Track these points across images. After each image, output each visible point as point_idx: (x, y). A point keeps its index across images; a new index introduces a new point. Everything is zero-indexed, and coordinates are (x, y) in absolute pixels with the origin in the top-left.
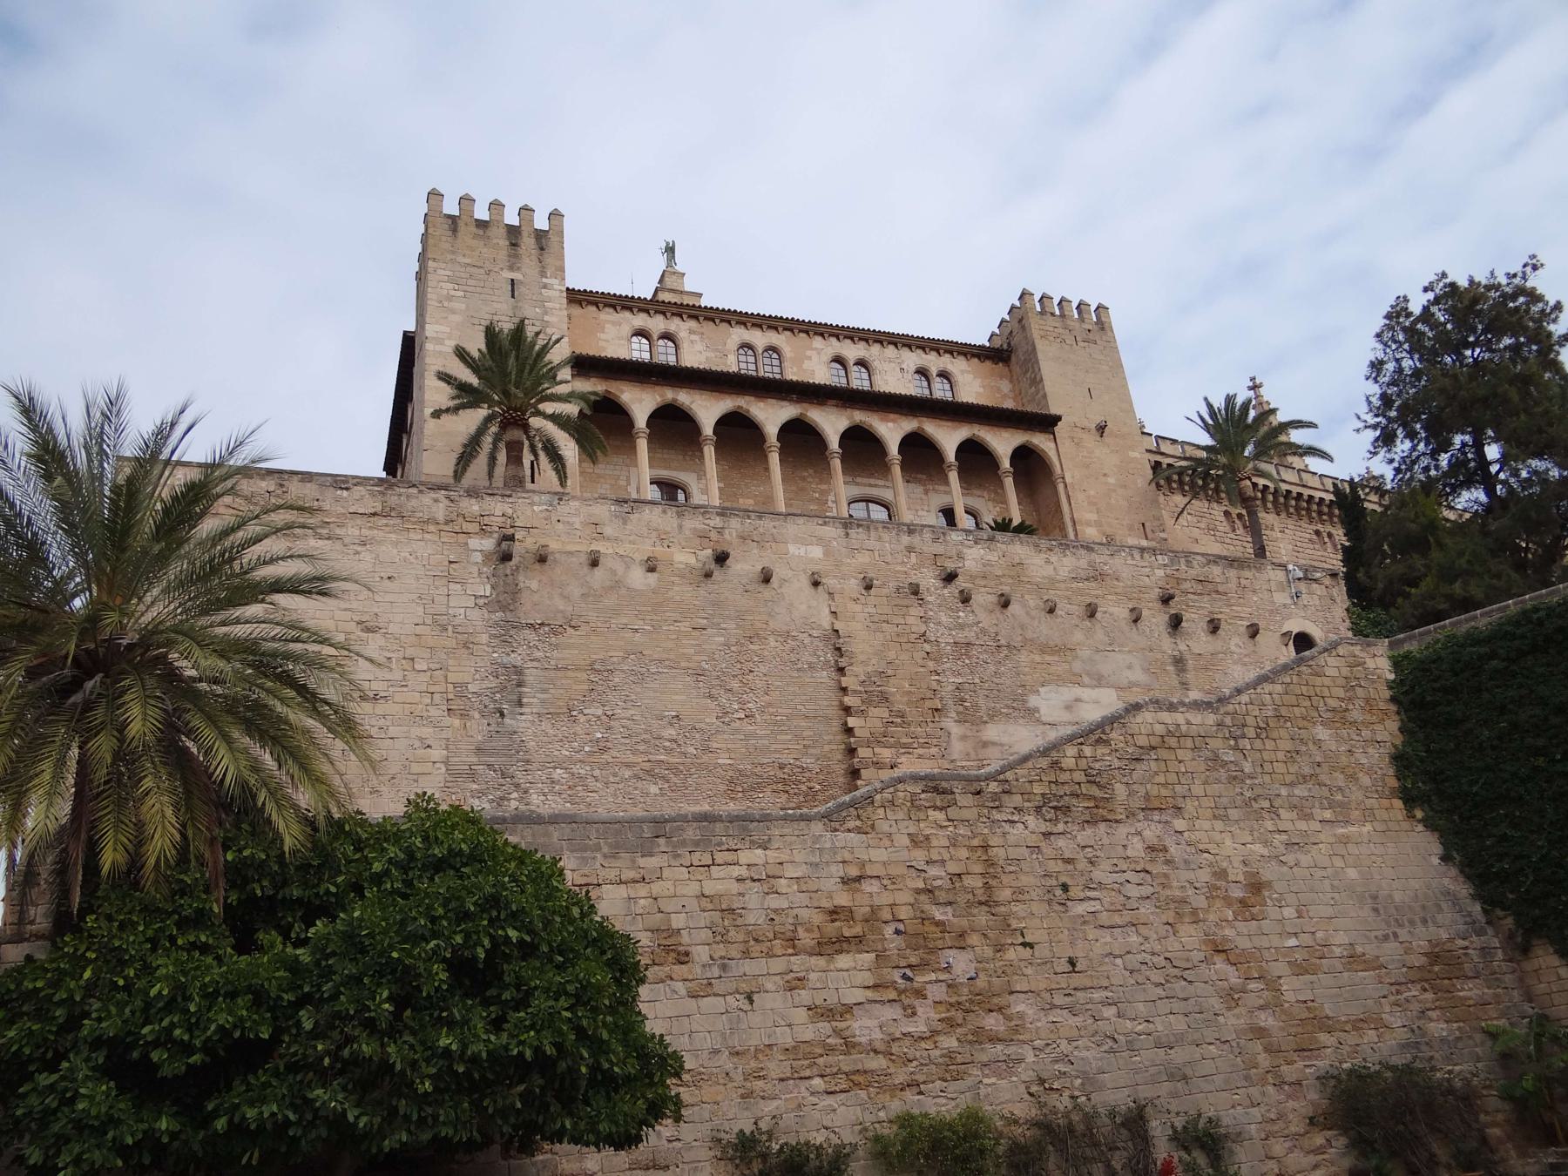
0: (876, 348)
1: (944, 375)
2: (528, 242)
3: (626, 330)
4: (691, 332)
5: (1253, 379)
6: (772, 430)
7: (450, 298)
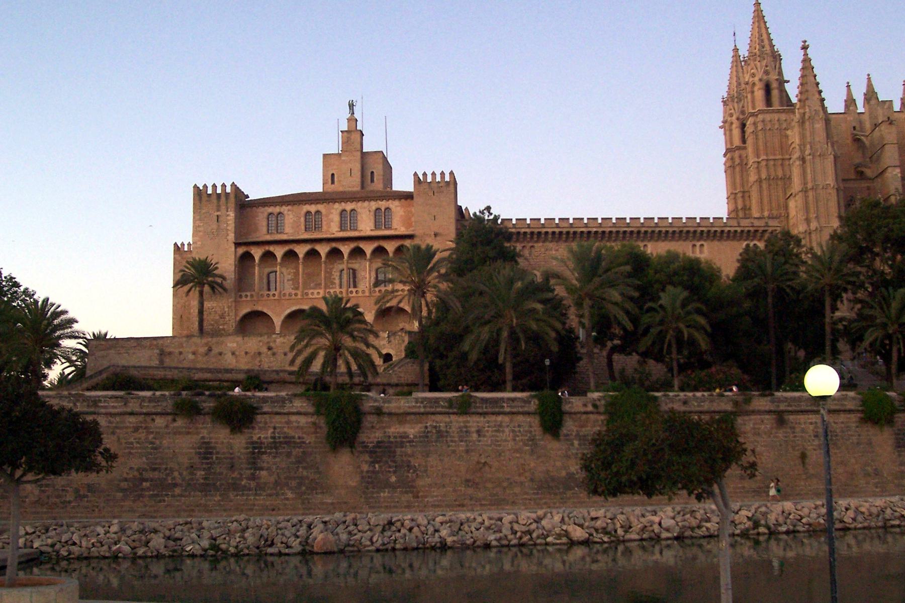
0: (360, 204)
1: (387, 209)
2: (223, 198)
3: (266, 214)
4: (289, 210)
5: (805, 42)
6: (301, 256)
7: (199, 226)
